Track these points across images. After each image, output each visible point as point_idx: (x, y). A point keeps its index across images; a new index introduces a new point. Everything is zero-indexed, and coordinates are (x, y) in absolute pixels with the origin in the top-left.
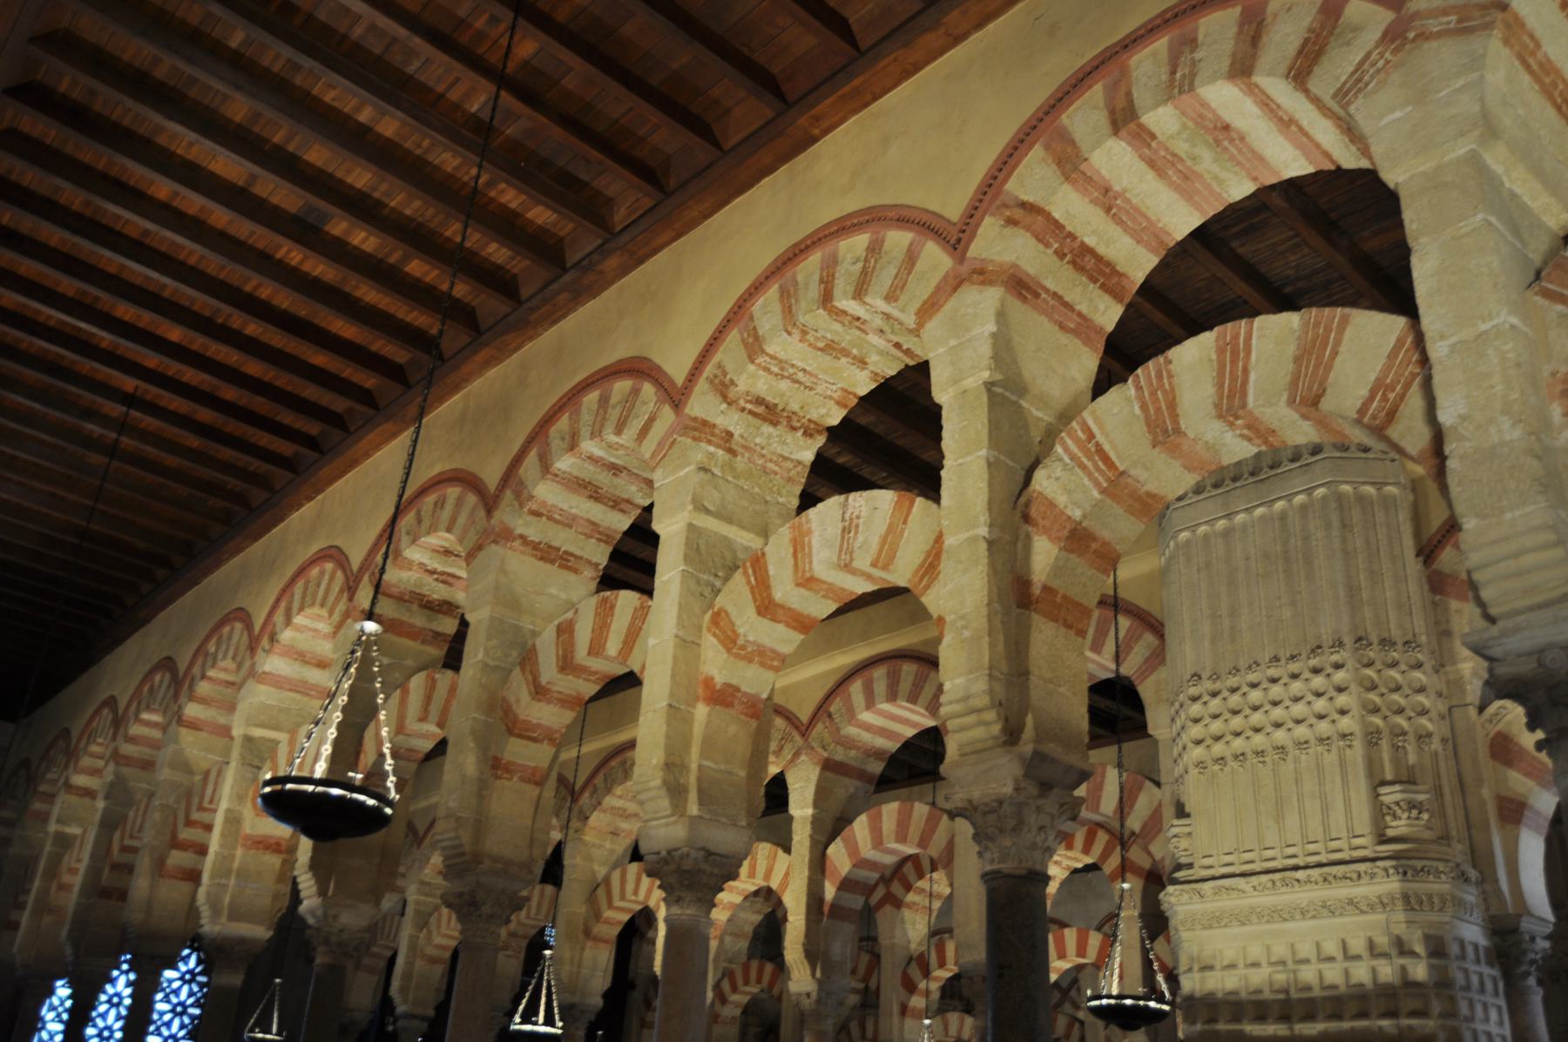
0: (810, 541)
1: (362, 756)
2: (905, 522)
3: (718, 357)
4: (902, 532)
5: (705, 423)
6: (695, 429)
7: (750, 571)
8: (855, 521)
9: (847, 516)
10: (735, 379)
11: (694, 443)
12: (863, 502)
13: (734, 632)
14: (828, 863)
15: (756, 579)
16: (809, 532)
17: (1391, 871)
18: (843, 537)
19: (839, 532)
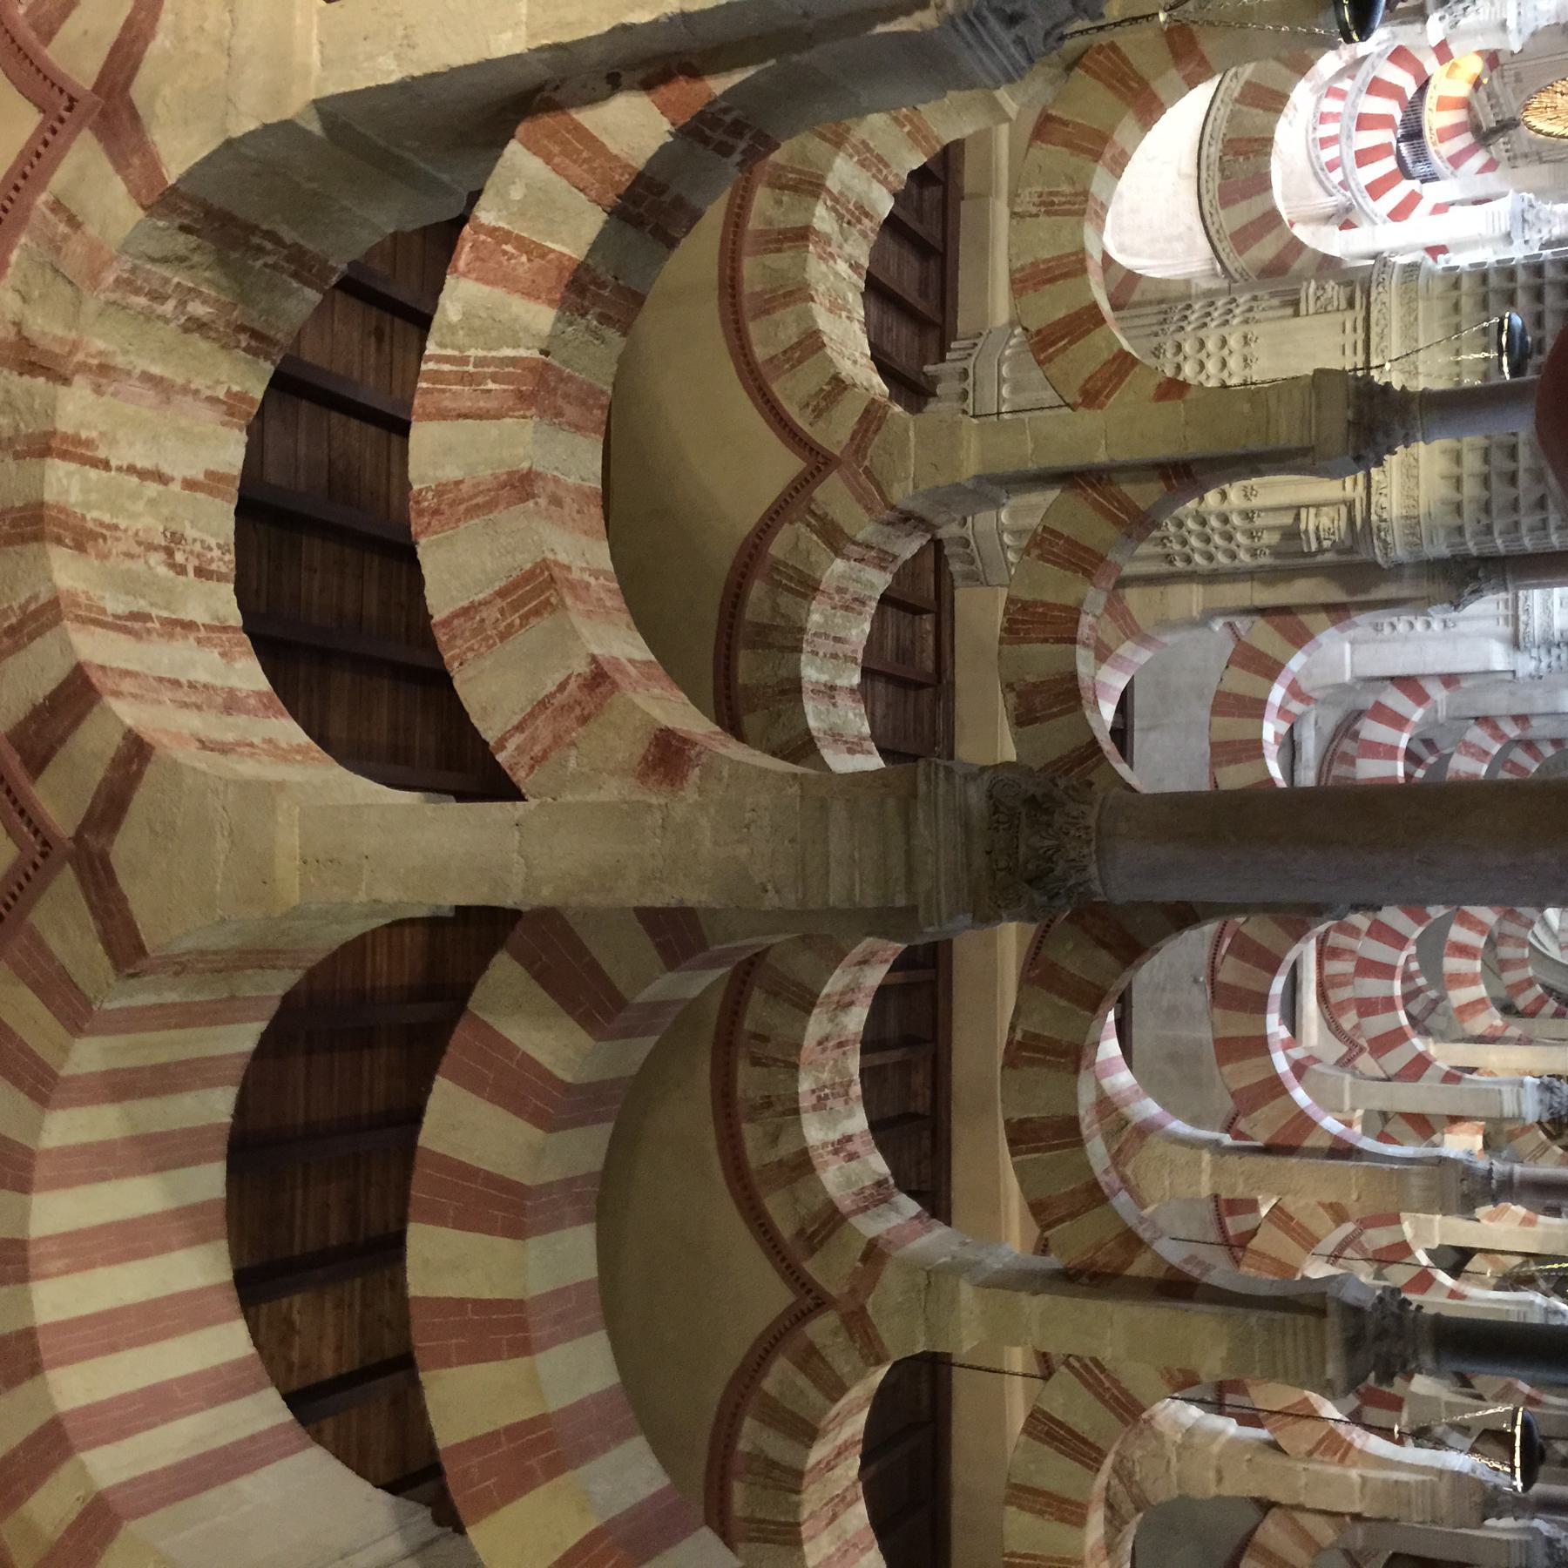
0: (1045, 261)
1: (1101, 1259)
2: (1065, 123)
3: (792, 410)
4: (1076, 125)
5: (867, 411)
6: (866, 431)
7: (1051, 350)
8: (1044, 198)
9: (1034, 210)
10: (832, 371)
11: (884, 428)
12: (1028, 190)
13: (1114, 359)
14: (1279, 1141)
15: (1062, 338)
16: (1034, 264)
17: (1381, 289)
18: (1056, 213)
19: (1048, 219)
